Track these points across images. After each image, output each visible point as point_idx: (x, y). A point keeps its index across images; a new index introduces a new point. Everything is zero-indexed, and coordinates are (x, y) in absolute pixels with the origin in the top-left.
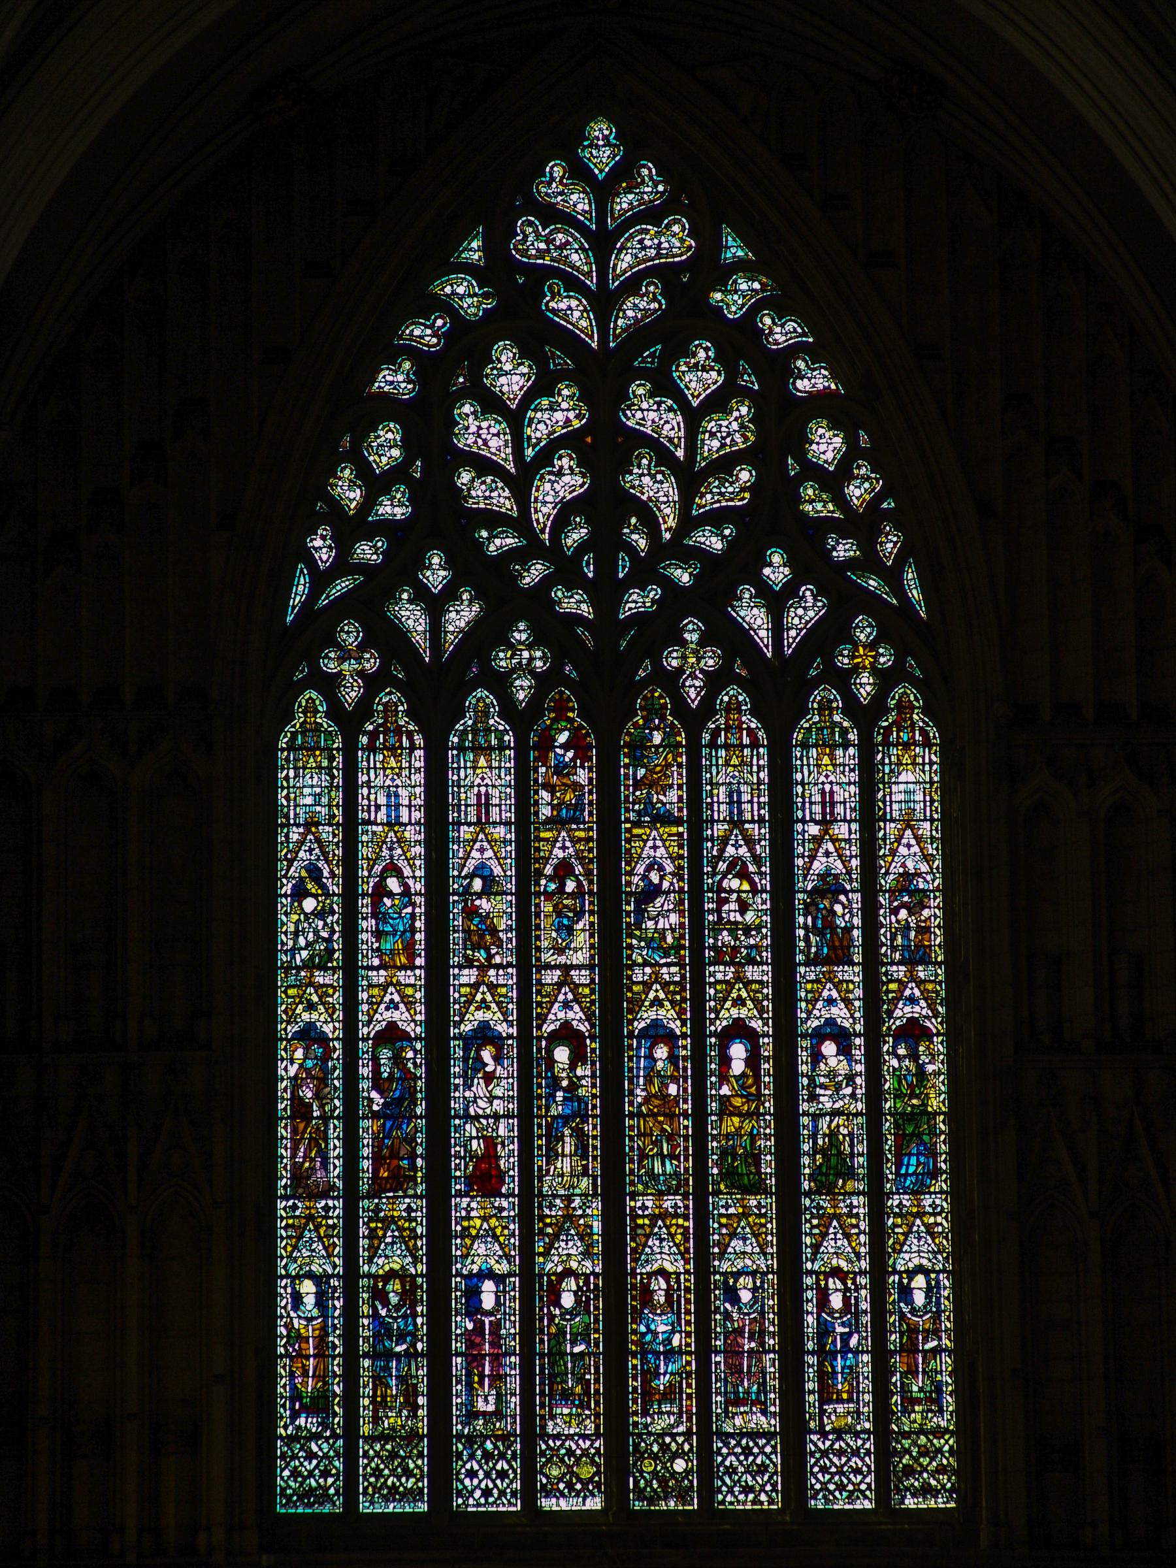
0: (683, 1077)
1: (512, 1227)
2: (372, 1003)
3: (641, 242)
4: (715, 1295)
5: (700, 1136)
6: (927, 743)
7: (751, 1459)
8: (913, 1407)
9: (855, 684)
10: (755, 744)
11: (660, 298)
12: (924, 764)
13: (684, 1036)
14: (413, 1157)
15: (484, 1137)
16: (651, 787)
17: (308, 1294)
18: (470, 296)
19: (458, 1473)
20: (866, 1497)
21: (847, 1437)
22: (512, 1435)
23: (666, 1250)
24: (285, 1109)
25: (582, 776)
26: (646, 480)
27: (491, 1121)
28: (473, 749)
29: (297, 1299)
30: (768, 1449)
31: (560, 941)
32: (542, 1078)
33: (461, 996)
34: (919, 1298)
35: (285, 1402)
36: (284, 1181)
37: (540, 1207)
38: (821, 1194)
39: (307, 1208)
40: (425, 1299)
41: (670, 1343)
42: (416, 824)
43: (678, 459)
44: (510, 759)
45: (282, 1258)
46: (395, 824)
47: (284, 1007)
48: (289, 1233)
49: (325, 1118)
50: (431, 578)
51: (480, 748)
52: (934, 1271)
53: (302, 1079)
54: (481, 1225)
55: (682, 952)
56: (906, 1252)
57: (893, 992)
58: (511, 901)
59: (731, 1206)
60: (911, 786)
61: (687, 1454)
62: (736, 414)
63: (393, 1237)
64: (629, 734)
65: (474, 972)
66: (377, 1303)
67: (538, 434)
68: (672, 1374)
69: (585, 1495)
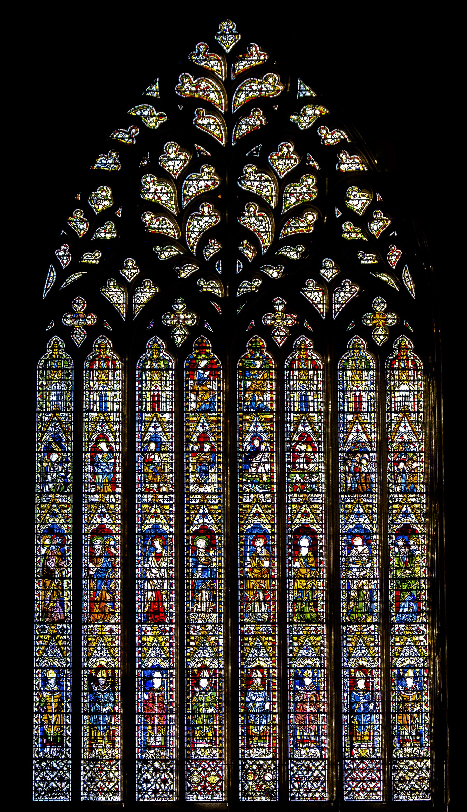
0: (272, 557)
1: (171, 641)
2: (90, 513)
3: (250, 87)
4: (290, 681)
6: (416, 369)
7: (310, 773)
8: (406, 744)
9: (374, 335)
11: (261, 118)
12: (414, 380)
13: (273, 533)
14: (114, 601)
15: (155, 590)
16: (254, 391)
17: (52, 678)
18: (151, 116)
19: (139, 780)
20: (377, 795)
21: (367, 762)
22: (170, 759)
23: (261, 655)
24: (39, 573)
25: (214, 385)
26: (253, 220)
27: (159, 581)
28: (150, 370)
29: (45, 680)
30: (321, 768)
31: (201, 479)
32: (190, 557)
33: (142, 510)
34: (410, 683)
35: (38, 739)
36: (38, 614)
37: (188, 630)
38: (352, 624)
39: (51, 629)
40: (120, 681)
41: (263, 707)
42: (116, 412)
43: (271, 207)
44: (172, 375)
45: (37, 657)
46: (105, 412)
47: (38, 515)
48: (41, 643)
49: (62, 579)
50: (127, 274)
51: (156, 370)
52: (418, 668)
53: (49, 556)
54: (153, 640)
55: (272, 486)
56: (402, 657)
57: (396, 509)
58: (172, 456)
59: (300, 631)
60: (407, 393)
61: (272, 770)
62: (305, 183)
63: (102, 646)
64: (241, 362)
65: (150, 496)
66: (92, 683)
67: (190, 194)
68: (264, 725)
69: (213, 794)
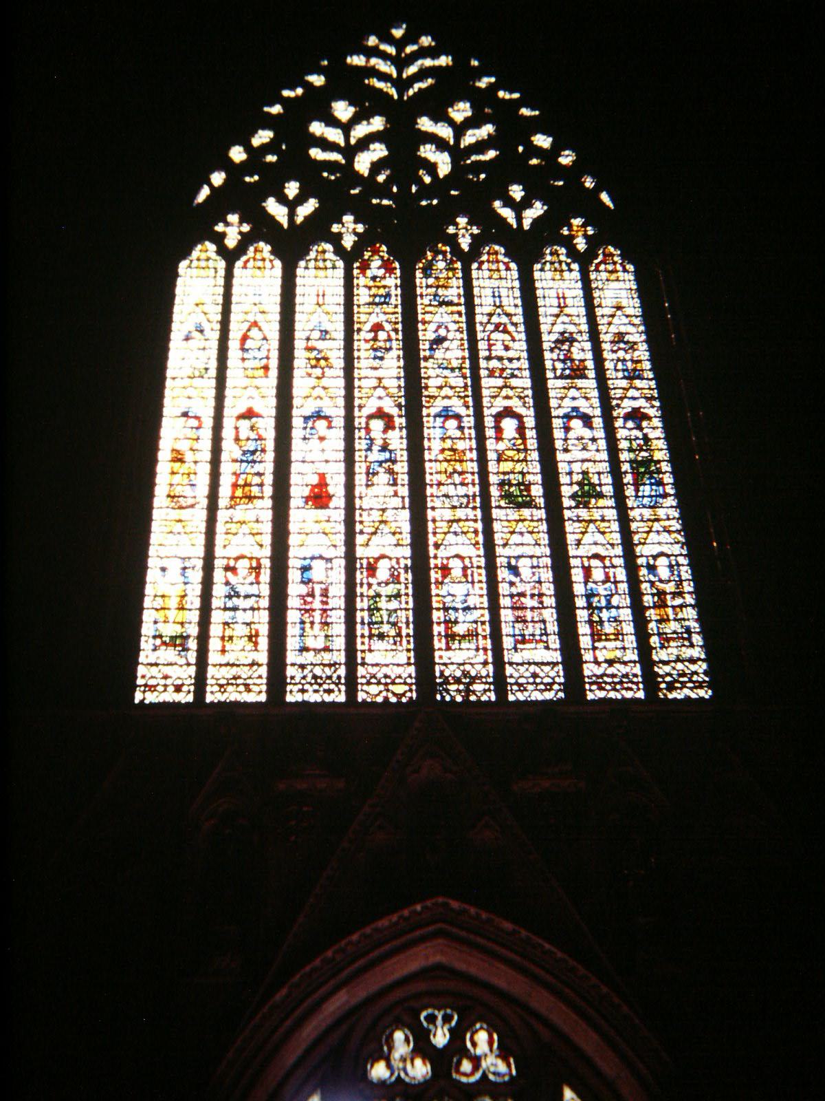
5: (483, 473)
10: (508, 269)
14: (261, 485)
21: (617, 665)
34: (664, 572)
55: (464, 371)
